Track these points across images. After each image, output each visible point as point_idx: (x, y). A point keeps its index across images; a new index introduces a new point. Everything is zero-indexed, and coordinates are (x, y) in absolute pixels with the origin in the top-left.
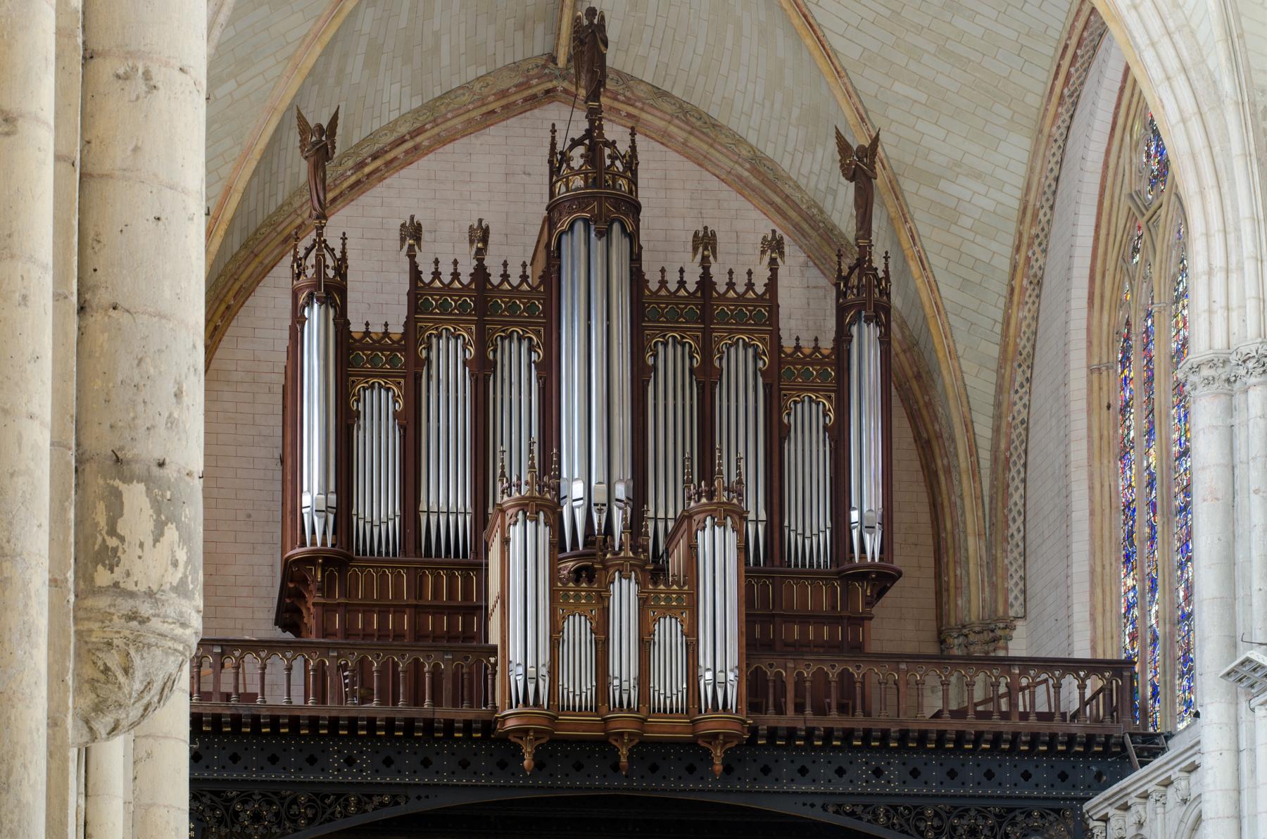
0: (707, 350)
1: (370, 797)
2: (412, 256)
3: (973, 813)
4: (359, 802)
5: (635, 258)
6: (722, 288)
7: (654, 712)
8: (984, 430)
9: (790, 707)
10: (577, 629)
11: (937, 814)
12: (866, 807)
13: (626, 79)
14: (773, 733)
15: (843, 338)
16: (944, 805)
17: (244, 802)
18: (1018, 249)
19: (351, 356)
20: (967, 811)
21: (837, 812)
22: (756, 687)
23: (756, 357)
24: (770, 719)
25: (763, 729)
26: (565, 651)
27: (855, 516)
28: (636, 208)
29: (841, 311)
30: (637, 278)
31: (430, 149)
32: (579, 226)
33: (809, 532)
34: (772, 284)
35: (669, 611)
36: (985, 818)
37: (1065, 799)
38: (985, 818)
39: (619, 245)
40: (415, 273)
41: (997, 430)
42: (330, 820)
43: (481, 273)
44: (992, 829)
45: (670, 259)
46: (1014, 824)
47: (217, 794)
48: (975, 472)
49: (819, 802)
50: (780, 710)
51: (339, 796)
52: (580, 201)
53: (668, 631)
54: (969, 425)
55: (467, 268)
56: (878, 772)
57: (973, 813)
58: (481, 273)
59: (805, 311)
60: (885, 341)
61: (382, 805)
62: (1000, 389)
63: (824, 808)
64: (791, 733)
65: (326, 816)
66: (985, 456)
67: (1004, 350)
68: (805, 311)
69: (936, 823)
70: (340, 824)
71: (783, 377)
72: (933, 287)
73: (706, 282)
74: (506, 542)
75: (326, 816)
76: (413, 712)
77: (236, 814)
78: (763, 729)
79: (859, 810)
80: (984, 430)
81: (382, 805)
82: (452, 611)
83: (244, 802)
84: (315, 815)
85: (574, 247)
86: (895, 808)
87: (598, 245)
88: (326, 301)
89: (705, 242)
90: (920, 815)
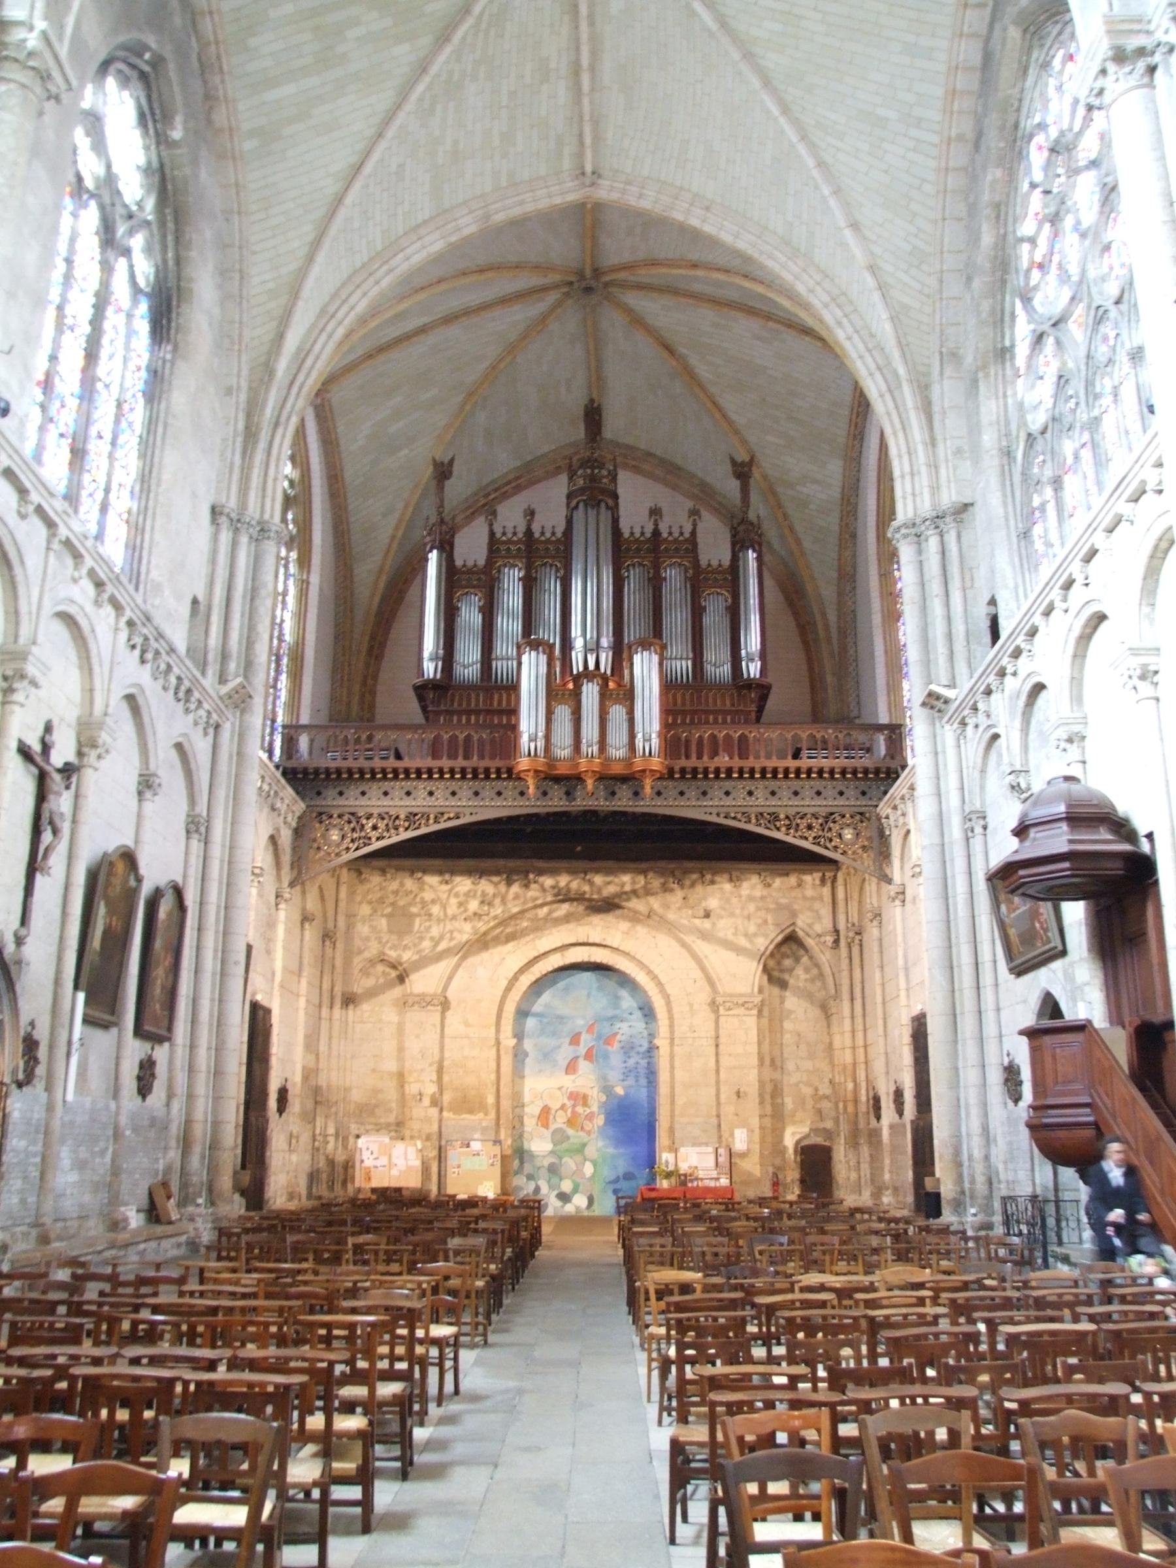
0: (656, 567)
2: (491, 525)
5: (615, 521)
6: (665, 535)
7: (608, 759)
8: (832, 617)
9: (694, 756)
10: (563, 712)
14: (683, 771)
15: (735, 559)
16: (791, 812)
19: (454, 581)
22: (672, 745)
23: (686, 571)
24: (683, 762)
25: (677, 768)
26: (556, 726)
27: (743, 652)
28: (615, 497)
29: (733, 545)
31: (526, 487)
32: (581, 505)
33: (718, 667)
34: (693, 533)
35: (617, 701)
39: (605, 516)
40: (492, 534)
41: (839, 617)
43: (529, 532)
45: (634, 517)
47: (353, 814)
48: (829, 639)
49: (715, 811)
50: (688, 757)
52: (582, 490)
53: (617, 712)
54: (824, 615)
55: (521, 529)
56: (750, 793)
58: (529, 532)
59: (715, 548)
60: (759, 559)
64: (695, 771)
67: (839, 570)
68: (715, 548)
70: (424, 830)
71: (699, 581)
72: (798, 542)
73: (656, 533)
76: (465, 763)
78: (677, 768)
80: (832, 617)
82: (501, 712)
85: (579, 515)
87: (592, 513)
88: (441, 549)
89: (655, 512)
90: (777, 818)
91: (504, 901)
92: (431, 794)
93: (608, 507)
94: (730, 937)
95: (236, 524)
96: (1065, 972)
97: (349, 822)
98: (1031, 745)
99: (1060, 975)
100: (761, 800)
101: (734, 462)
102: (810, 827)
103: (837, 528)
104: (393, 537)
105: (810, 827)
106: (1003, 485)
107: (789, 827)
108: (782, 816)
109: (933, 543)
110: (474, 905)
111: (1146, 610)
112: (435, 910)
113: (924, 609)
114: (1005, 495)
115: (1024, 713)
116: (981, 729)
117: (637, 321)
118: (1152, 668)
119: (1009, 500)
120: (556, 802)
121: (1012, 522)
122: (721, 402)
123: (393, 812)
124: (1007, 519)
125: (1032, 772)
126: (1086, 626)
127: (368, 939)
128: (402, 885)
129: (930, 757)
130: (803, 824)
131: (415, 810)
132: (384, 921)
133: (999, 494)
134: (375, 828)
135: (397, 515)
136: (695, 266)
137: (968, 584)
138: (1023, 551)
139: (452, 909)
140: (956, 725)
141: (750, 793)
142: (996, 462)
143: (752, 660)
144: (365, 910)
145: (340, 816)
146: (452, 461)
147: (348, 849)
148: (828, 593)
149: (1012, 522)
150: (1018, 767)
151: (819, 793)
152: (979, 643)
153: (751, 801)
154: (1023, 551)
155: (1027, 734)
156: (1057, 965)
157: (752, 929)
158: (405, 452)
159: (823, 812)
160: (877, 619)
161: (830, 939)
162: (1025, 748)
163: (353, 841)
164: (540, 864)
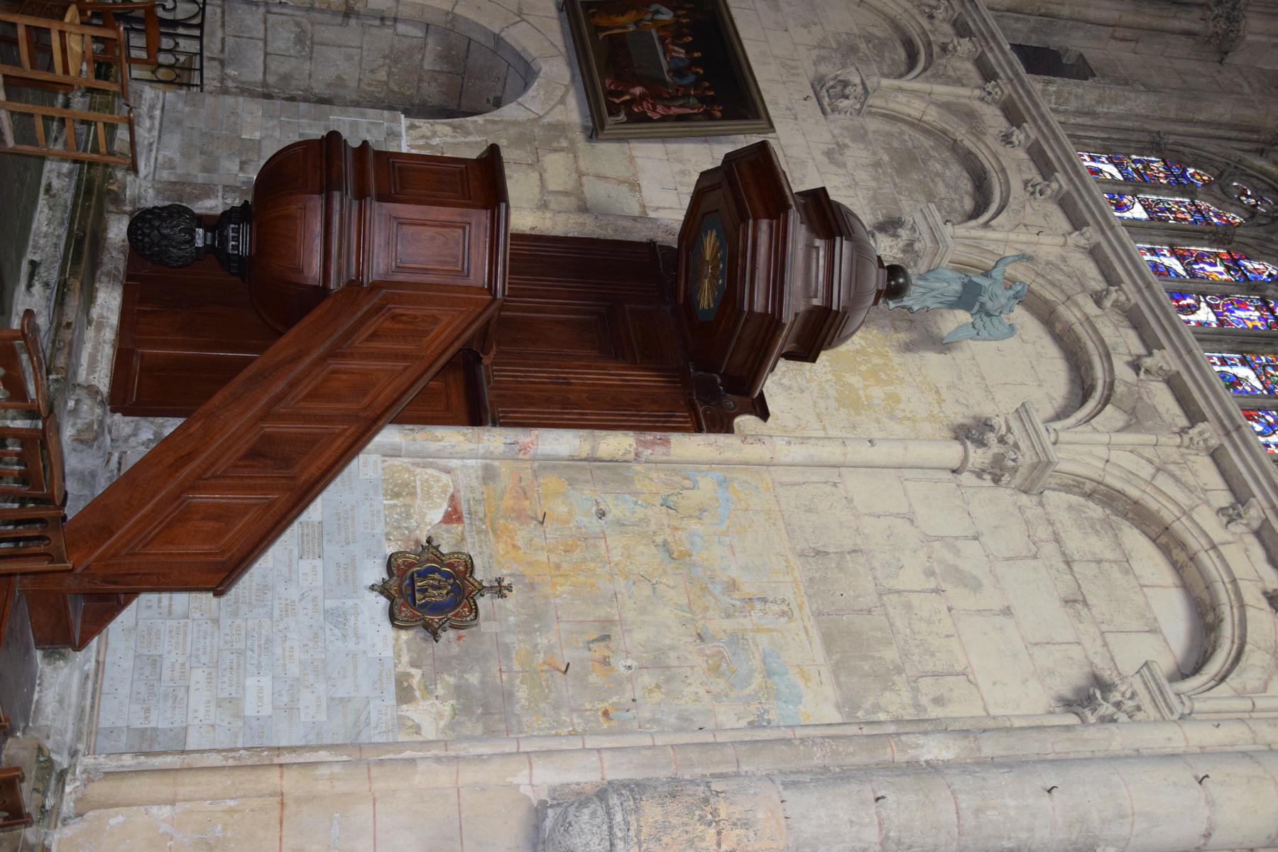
96: (559, 129)
98: (896, 128)
99: (557, 116)
106: (1234, 127)
111: (1089, 486)
114: (1220, 125)
115: (945, 132)
116: (926, 24)
118: (1006, 478)
119: (1211, 132)
121: (1180, 128)
125: (858, 121)
126: (1069, 329)
133: (1226, 118)
137: (1120, 33)
138: (1135, 136)
149: (1180, 129)
150: (870, 101)
152: (1033, 30)
154: (1135, 136)
155: (912, 125)
156: (572, 112)
162: (892, 118)
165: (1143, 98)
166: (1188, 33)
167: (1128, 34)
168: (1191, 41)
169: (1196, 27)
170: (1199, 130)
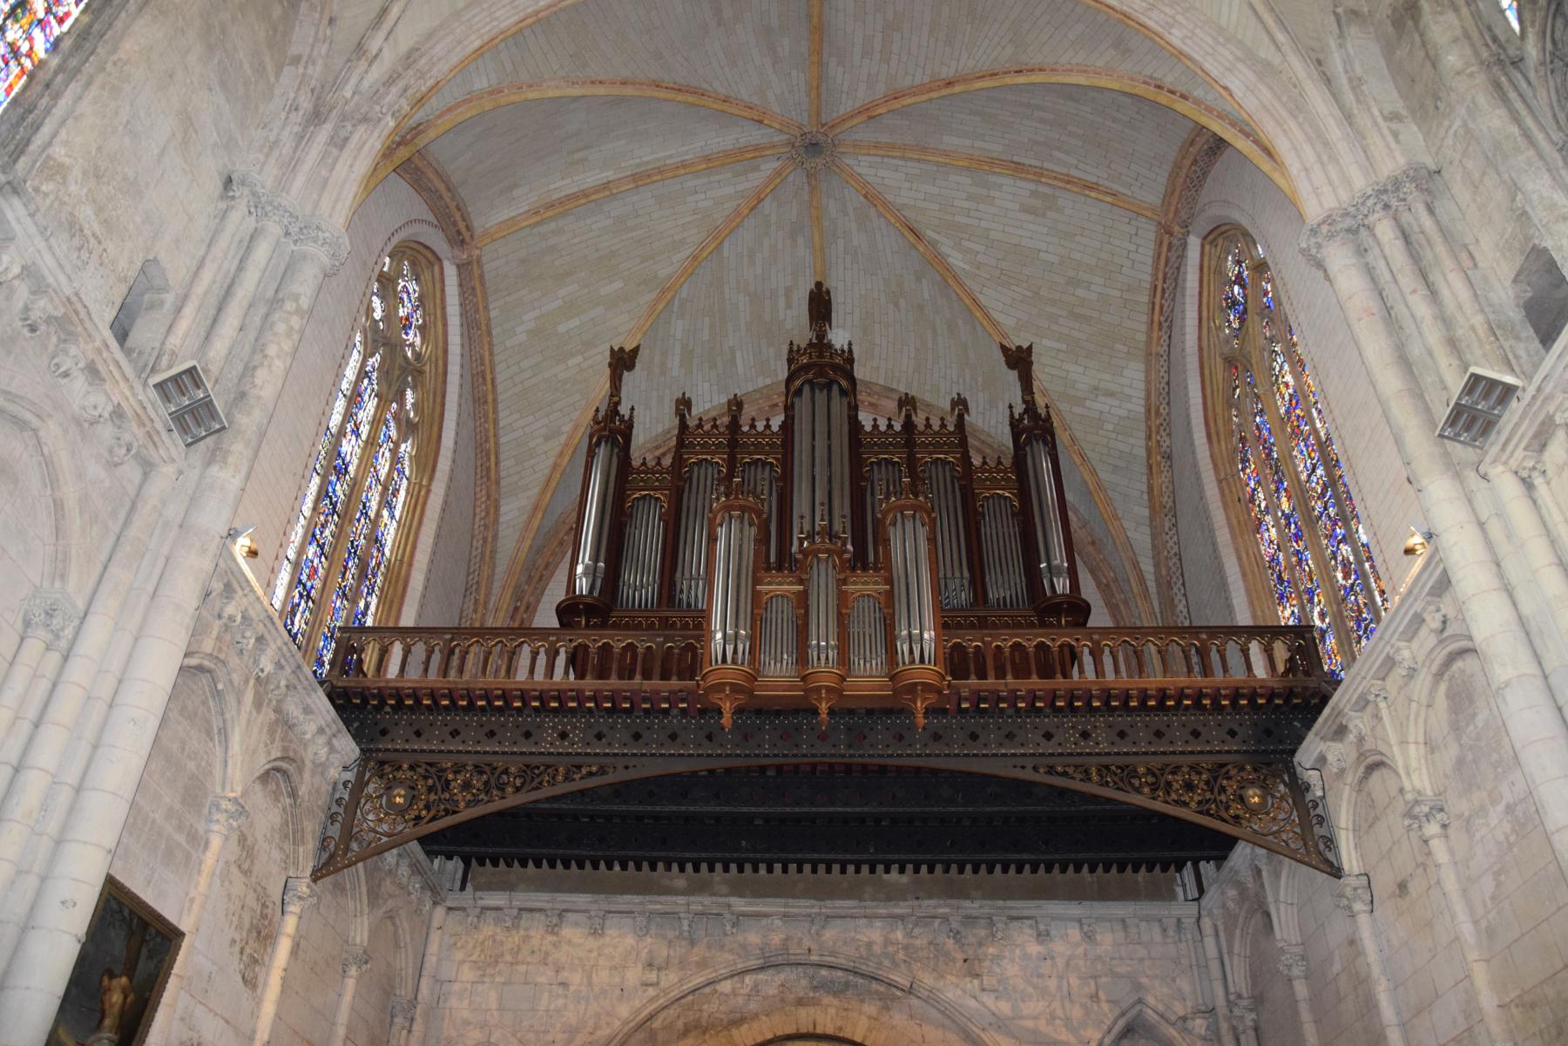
1: (579, 767)
3: (1185, 769)
4: (568, 772)
8: (1147, 567)
9: (991, 673)
11: (1150, 771)
12: (1076, 767)
13: (867, 384)
16: (1156, 762)
17: (456, 773)
18: (1149, 438)
20: (1179, 767)
21: (1049, 773)
22: (957, 662)
25: (965, 693)
30: (855, 425)
32: (807, 389)
36: (1199, 773)
37: (1274, 752)
38: (1199, 773)
39: (839, 405)
41: (1157, 565)
42: (537, 788)
44: (1207, 783)
46: (1229, 778)
49: (1029, 763)
51: (548, 767)
54: (1136, 565)
57: (1185, 769)
61: (590, 774)
62: (1154, 536)
63: (1035, 769)
65: (534, 784)
66: (1152, 585)
67: (1152, 508)
69: (1150, 779)
72: (1094, 472)
74: (713, 539)
75: (534, 784)
77: (448, 783)
79: (1070, 770)
80: (1147, 567)
81: (590, 774)
83: (456, 773)
84: (523, 784)
85: (803, 406)
86: (1107, 767)
87: (821, 397)
90: (1134, 774)
91: (682, 964)
92: (563, 736)
93: (843, 392)
94: (1042, 1025)
95: (259, 207)
97: (426, 778)
100: (1103, 741)
101: (1004, 349)
102: (1189, 786)
103: (1142, 453)
104: (555, 466)
105: (1189, 786)
107: (1154, 787)
108: (1141, 770)
109: (1385, 230)
110: (633, 975)
112: (576, 979)
113: (1391, 320)
117: (872, 197)
120: (768, 749)
122: (982, 299)
123: (500, 763)
124: (1527, 135)
127: (467, 1023)
128: (527, 938)
129: (1472, 531)
130: (1178, 781)
131: (535, 761)
132: (493, 995)
134: (467, 786)
135: (563, 438)
136: (949, 84)
139: (602, 977)
140: (1520, 453)
141: (1085, 735)
142: (1481, 78)
143: (1059, 575)
144: (468, 974)
145: (412, 768)
146: (636, 351)
147: (418, 818)
148: (1141, 538)
151: (1196, 734)
152: (1517, 338)
153: (1086, 747)
157: (1077, 1012)
158: (579, 359)
159: (1206, 762)
160: (1223, 536)
161: (1199, 1025)
163: (427, 807)
164: (740, 904)
165: (1530, 186)
166: (1431, 210)
167: (1464, 256)
168: (1436, 204)
169: (1420, 209)
170: (1529, 122)
